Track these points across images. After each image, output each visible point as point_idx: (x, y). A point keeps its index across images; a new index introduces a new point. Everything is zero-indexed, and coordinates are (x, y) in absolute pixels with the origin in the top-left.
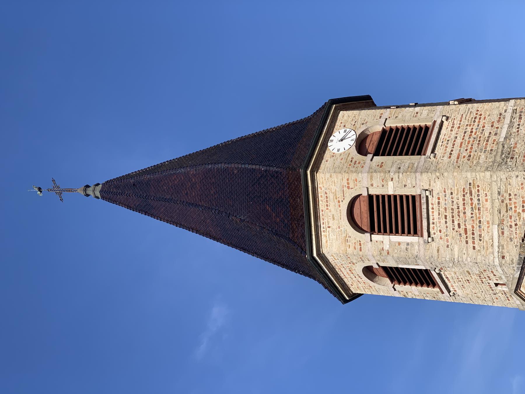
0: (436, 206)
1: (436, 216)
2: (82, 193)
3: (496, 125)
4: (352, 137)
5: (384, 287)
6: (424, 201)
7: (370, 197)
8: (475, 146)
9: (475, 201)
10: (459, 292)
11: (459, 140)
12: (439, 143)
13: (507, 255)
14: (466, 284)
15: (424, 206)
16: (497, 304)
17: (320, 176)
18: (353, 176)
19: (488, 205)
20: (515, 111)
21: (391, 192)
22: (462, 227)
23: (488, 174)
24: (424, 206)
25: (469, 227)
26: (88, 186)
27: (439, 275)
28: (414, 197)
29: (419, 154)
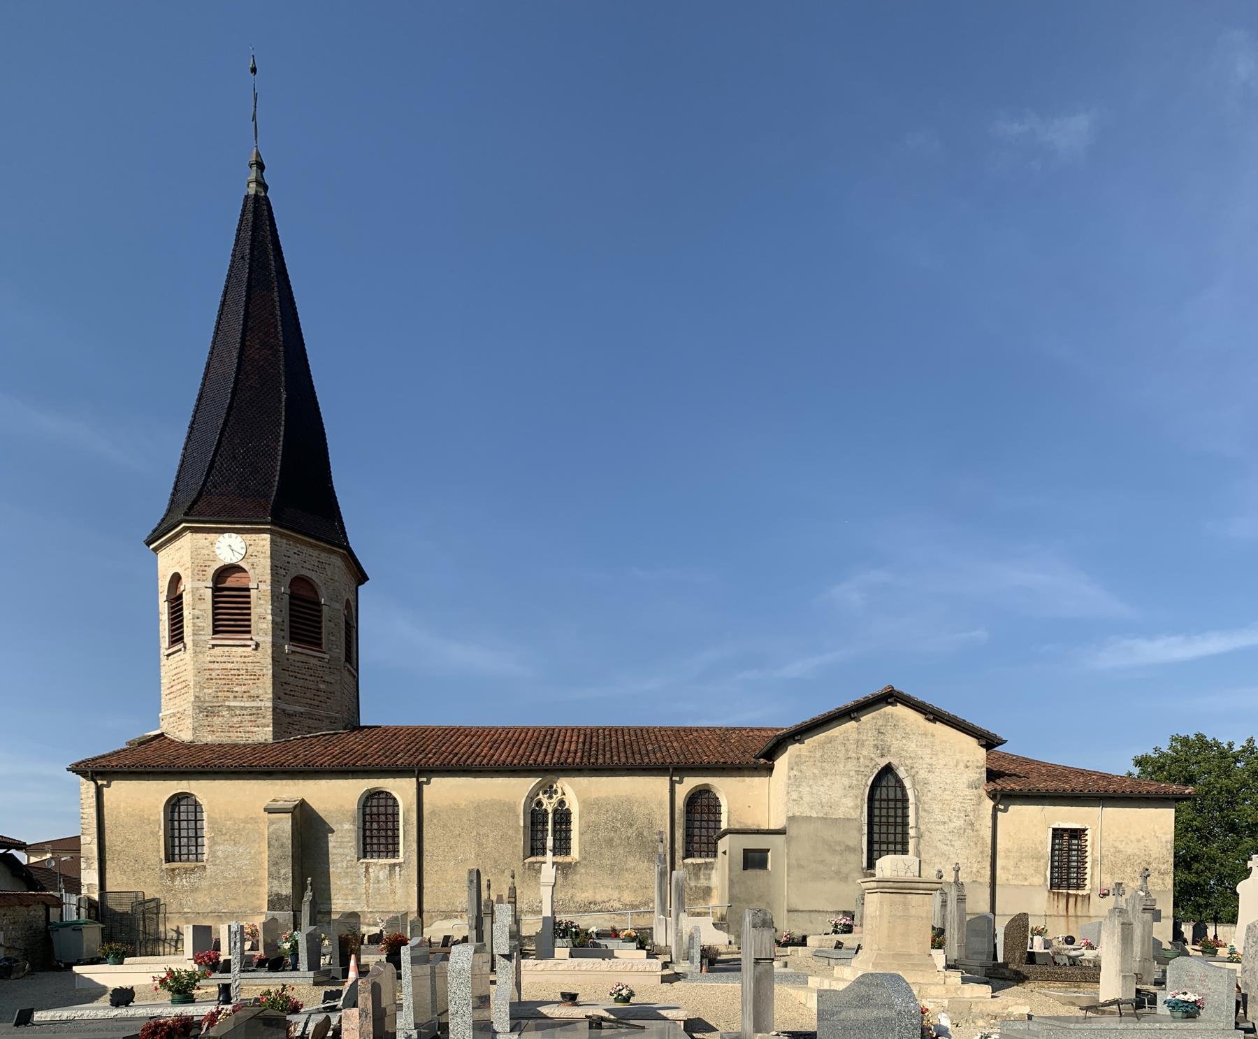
11: (230, 666)
29: (215, 632)
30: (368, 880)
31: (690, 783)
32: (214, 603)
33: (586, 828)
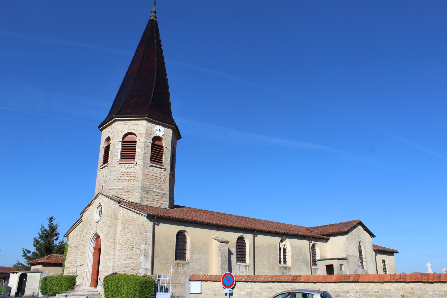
0: (131, 166)
1: (127, 167)
2: (153, 10)
3: (160, 188)
4: (160, 134)
5: (103, 144)
6: (133, 162)
7: (136, 142)
8: (152, 181)
9: (131, 181)
10: (101, 172)
11: (155, 175)
12: (154, 168)
13: (111, 191)
14: (103, 175)
15: (130, 162)
16: (96, 186)
17: (145, 122)
18: (144, 135)
19: (130, 185)
20: (164, 194)
21: (137, 150)
22: (122, 176)
23: (141, 185)
24: (130, 162)
25: (122, 178)
26: (155, 12)
27: (106, 166)
28: (134, 158)
29: (151, 160)
30: (239, 272)
31: (313, 242)
32: (152, 149)
33: (293, 255)
